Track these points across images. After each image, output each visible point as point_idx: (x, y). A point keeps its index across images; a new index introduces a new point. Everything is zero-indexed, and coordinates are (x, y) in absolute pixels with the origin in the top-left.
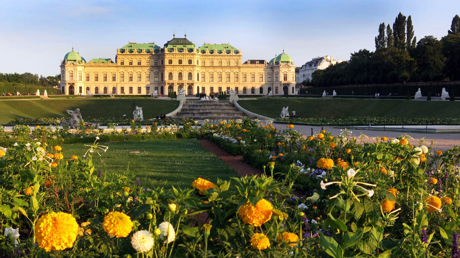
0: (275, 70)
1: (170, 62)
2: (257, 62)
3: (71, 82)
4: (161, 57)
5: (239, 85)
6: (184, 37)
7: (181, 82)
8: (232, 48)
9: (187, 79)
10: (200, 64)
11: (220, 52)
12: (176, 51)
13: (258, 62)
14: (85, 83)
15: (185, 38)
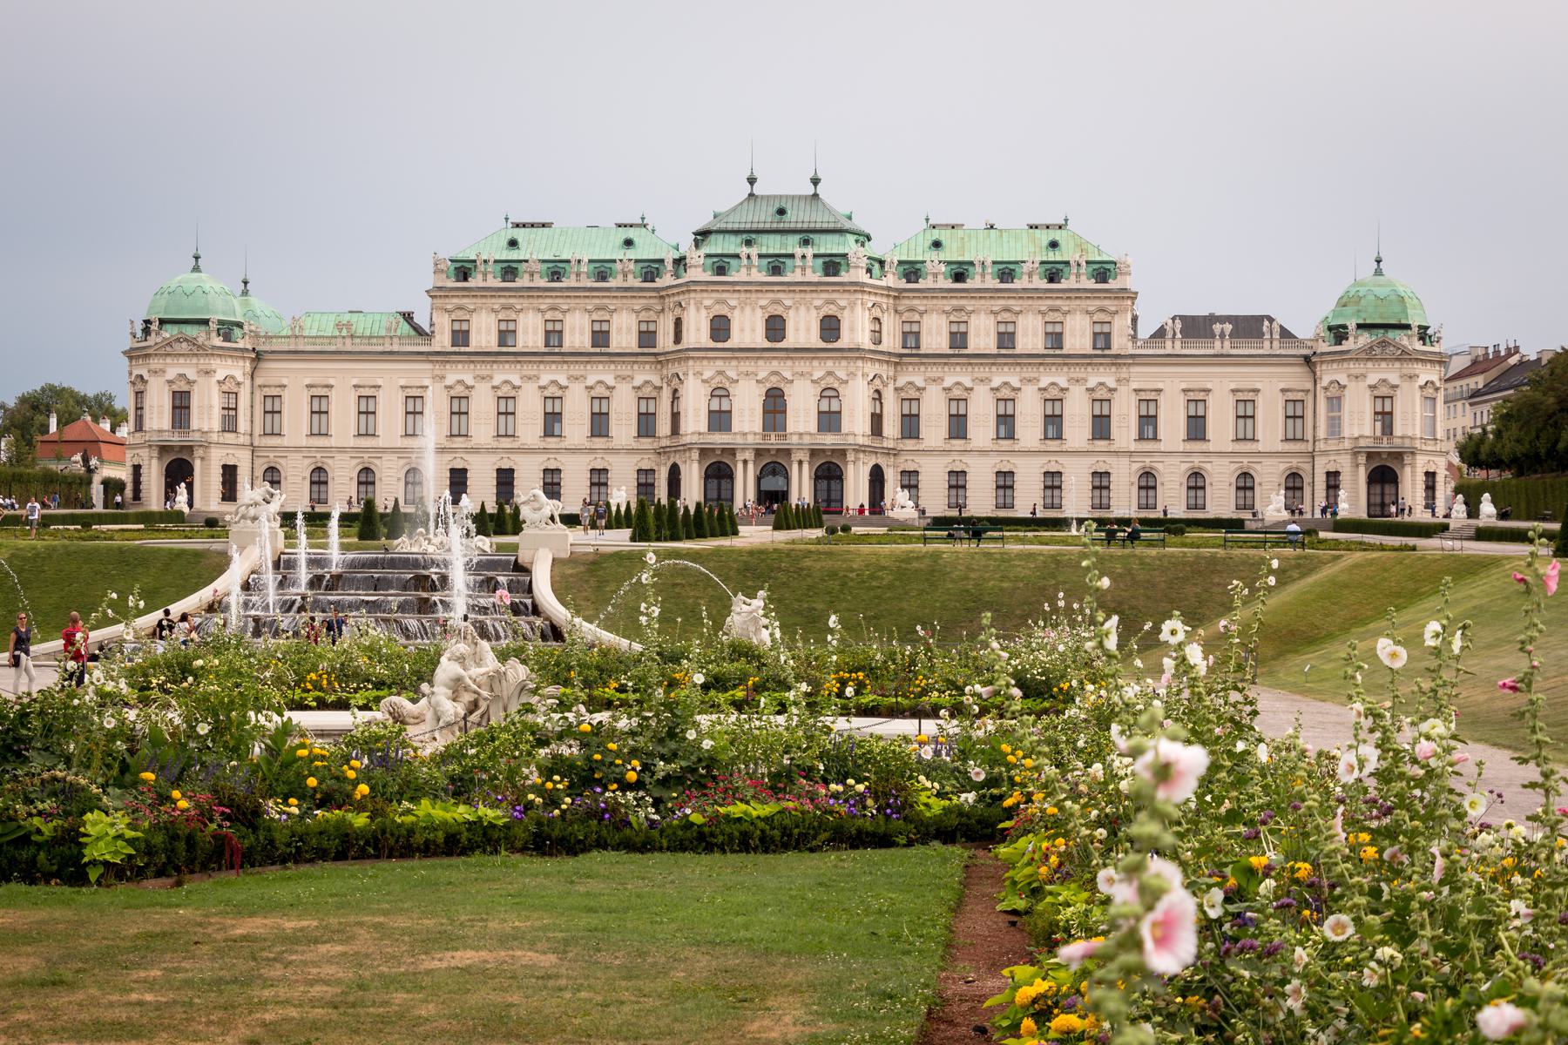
0: (1327, 375)
1: (720, 328)
2: (1217, 327)
3: (176, 438)
4: (670, 302)
5: (1112, 460)
6: (810, 190)
7: (773, 441)
8: (1081, 247)
9: (813, 427)
10: (891, 342)
11: (1007, 272)
12: (749, 272)
13: (1228, 327)
14: (254, 449)
15: (815, 196)
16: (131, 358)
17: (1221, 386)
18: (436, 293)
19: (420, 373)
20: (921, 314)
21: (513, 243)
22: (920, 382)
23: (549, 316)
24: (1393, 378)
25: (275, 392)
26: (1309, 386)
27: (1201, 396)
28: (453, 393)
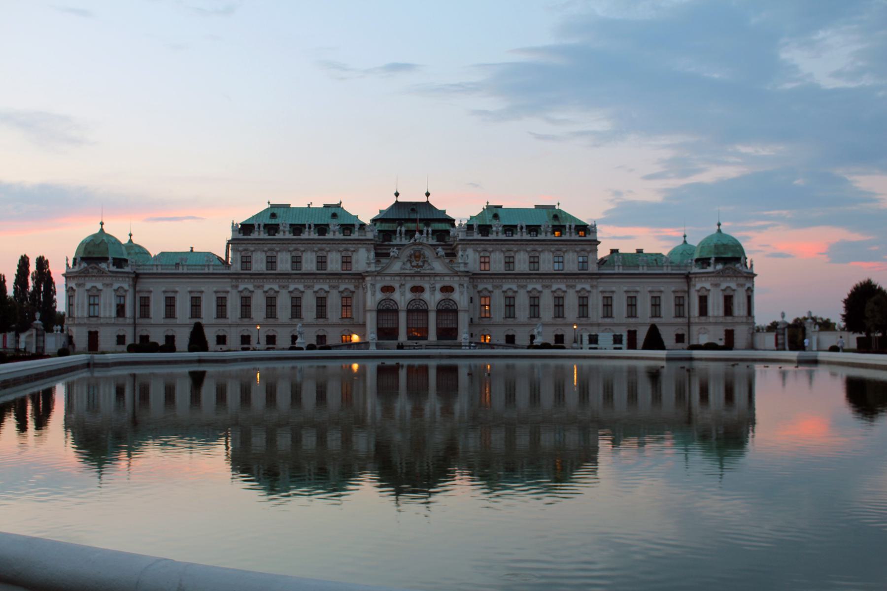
0: (699, 284)
11: (533, 229)
14: (135, 325)
16: (66, 278)
17: (644, 291)
18: (233, 243)
19: (225, 285)
20: (490, 252)
21: (273, 216)
22: (490, 288)
23: (294, 254)
24: (733, 285)
25: (145, 295)
26: (686, 289)
27: (632, 294)
28: (243, 295)
